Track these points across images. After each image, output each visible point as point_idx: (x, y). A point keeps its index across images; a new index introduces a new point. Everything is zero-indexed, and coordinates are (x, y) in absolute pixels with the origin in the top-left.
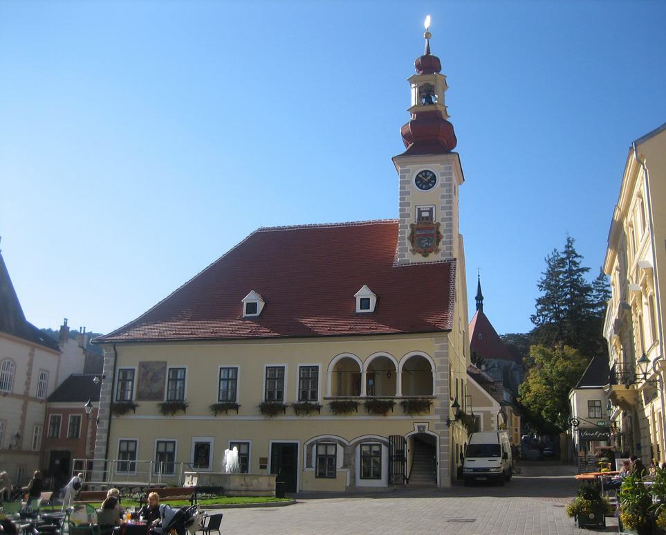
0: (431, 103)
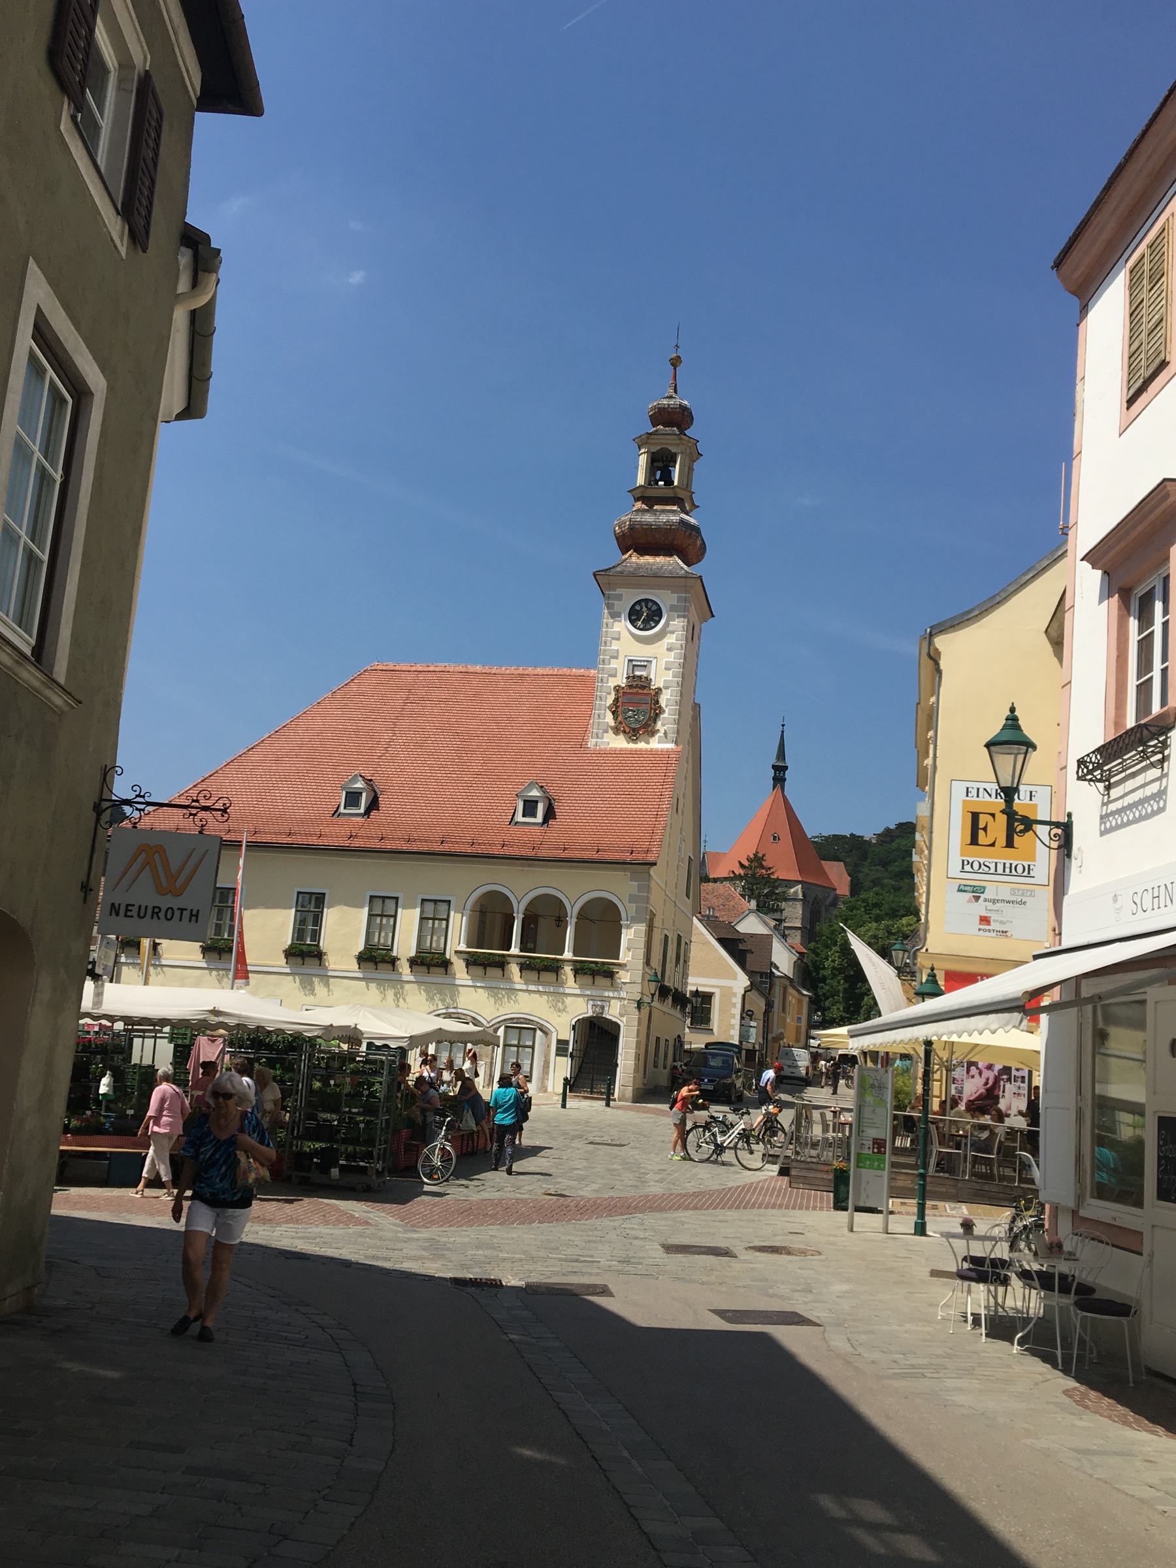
0: (669, 482)
